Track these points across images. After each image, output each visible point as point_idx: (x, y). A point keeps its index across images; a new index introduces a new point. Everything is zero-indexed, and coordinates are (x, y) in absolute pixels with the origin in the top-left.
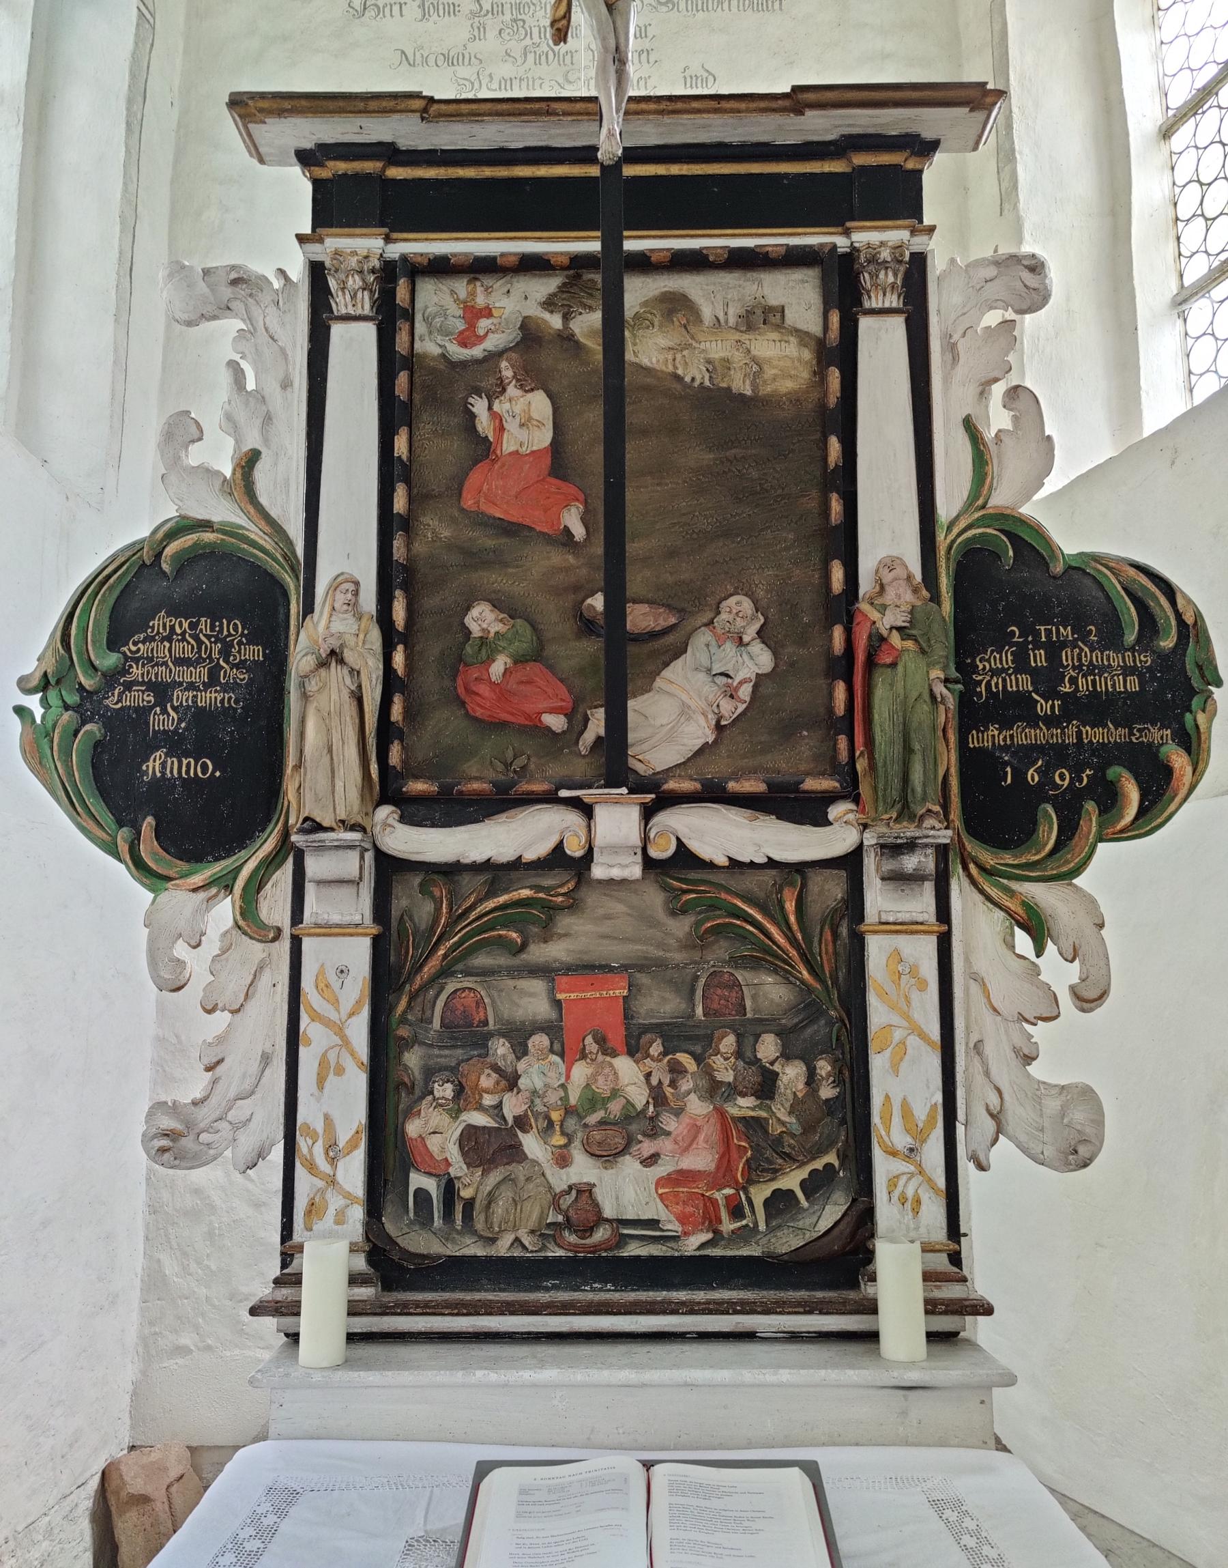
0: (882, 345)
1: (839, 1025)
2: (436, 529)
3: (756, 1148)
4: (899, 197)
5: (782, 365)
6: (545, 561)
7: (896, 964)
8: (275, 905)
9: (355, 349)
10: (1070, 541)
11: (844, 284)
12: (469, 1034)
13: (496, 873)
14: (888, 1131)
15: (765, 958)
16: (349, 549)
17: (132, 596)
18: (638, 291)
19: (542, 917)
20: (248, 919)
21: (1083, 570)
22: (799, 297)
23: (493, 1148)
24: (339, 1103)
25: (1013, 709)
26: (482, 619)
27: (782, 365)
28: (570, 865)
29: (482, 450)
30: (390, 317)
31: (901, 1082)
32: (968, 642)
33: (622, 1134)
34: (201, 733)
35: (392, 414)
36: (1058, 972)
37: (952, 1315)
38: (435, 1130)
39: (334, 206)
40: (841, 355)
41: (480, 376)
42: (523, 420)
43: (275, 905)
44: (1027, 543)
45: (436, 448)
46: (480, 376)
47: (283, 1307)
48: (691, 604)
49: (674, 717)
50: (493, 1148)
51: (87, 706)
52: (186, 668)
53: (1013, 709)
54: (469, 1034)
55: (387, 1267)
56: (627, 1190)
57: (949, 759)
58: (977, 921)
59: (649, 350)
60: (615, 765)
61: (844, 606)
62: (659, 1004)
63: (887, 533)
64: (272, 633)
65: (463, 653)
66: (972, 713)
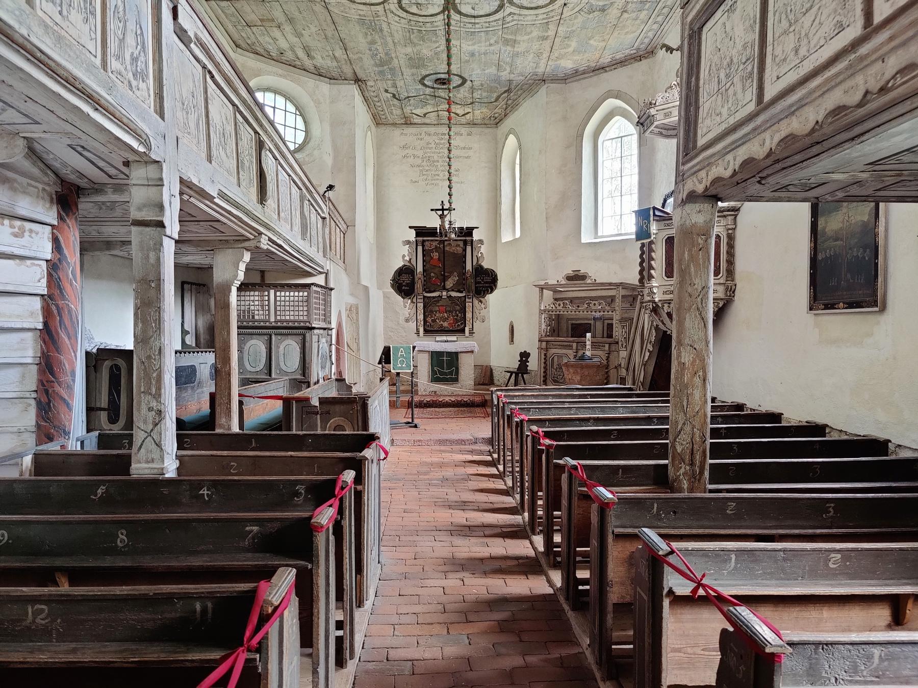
0: (469, 249)
1: (463, 311)
2: (428, 266)
3: (456, 321)
4: (471, 234)
5: (460, 250)
6: (437, 270)
7: (468, 305)
8: (414, 300)
9: (420, 248)
10: (485, 267)
11: (465, 243)
12: (432, 312)
13: (434, 297)
14: (467, 319)
15: (457, 305)
16: (420, 269)
17: (401, 272)
18: (446, 243)
19: (438, 301)
20: (412, 302)
21: (487, 269)
22: (461, 244)
23: (434, 321)
24: (421, 317)
25: (480, 283)
26: (432, 274)
27: (460, 250)
28: (440, 297)
29: (432, 258)
30: (423, 246)
31: (469, 315)
32: (476, 276)
33: (445, 320)
34: (407, 285)
35: (424, 255)
36: (483, 306)
37: (472, 333)
38: (429, 319)
39: (418, 235)
40: (465, 250)
41: (432, 251)
42: (436, 255)
43: (414, 300)
44: (481, 267)
45: (428, 258)
46: (432, 251)
47: (418, 333)
48: (451, 273)
49: (449, 284)
50: (434, 321)
51: (397, 282)
52: (405, 279)
53: (480, 283)
54: (432, 312)
55: (426, 331)
56: (445, 324)
57: (473, 288)
58: (476, 302)
59: (447, 249)
60: (444, 288)
61: (464, 274)
62: (448, 309)
63: (469, 267)
64: (413, 276)
65: (430, 278)
66: (476, 283)
